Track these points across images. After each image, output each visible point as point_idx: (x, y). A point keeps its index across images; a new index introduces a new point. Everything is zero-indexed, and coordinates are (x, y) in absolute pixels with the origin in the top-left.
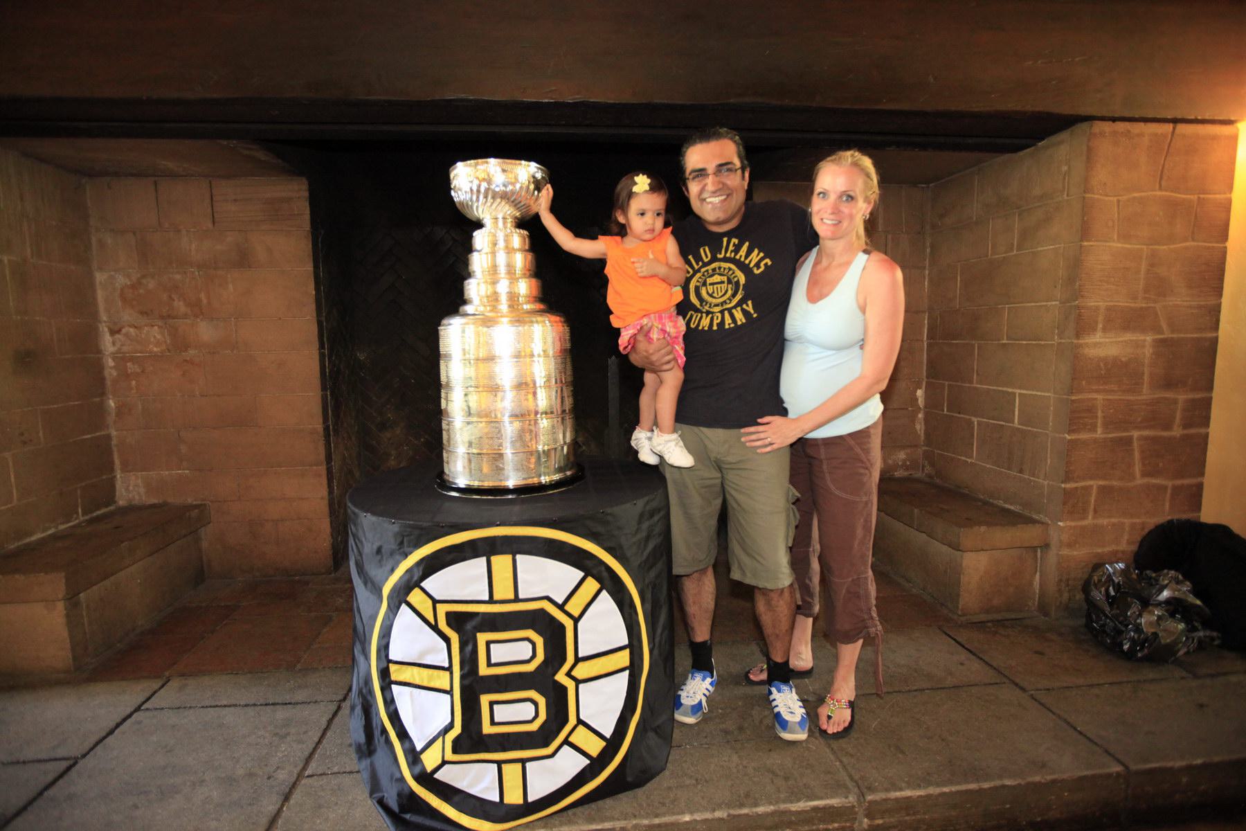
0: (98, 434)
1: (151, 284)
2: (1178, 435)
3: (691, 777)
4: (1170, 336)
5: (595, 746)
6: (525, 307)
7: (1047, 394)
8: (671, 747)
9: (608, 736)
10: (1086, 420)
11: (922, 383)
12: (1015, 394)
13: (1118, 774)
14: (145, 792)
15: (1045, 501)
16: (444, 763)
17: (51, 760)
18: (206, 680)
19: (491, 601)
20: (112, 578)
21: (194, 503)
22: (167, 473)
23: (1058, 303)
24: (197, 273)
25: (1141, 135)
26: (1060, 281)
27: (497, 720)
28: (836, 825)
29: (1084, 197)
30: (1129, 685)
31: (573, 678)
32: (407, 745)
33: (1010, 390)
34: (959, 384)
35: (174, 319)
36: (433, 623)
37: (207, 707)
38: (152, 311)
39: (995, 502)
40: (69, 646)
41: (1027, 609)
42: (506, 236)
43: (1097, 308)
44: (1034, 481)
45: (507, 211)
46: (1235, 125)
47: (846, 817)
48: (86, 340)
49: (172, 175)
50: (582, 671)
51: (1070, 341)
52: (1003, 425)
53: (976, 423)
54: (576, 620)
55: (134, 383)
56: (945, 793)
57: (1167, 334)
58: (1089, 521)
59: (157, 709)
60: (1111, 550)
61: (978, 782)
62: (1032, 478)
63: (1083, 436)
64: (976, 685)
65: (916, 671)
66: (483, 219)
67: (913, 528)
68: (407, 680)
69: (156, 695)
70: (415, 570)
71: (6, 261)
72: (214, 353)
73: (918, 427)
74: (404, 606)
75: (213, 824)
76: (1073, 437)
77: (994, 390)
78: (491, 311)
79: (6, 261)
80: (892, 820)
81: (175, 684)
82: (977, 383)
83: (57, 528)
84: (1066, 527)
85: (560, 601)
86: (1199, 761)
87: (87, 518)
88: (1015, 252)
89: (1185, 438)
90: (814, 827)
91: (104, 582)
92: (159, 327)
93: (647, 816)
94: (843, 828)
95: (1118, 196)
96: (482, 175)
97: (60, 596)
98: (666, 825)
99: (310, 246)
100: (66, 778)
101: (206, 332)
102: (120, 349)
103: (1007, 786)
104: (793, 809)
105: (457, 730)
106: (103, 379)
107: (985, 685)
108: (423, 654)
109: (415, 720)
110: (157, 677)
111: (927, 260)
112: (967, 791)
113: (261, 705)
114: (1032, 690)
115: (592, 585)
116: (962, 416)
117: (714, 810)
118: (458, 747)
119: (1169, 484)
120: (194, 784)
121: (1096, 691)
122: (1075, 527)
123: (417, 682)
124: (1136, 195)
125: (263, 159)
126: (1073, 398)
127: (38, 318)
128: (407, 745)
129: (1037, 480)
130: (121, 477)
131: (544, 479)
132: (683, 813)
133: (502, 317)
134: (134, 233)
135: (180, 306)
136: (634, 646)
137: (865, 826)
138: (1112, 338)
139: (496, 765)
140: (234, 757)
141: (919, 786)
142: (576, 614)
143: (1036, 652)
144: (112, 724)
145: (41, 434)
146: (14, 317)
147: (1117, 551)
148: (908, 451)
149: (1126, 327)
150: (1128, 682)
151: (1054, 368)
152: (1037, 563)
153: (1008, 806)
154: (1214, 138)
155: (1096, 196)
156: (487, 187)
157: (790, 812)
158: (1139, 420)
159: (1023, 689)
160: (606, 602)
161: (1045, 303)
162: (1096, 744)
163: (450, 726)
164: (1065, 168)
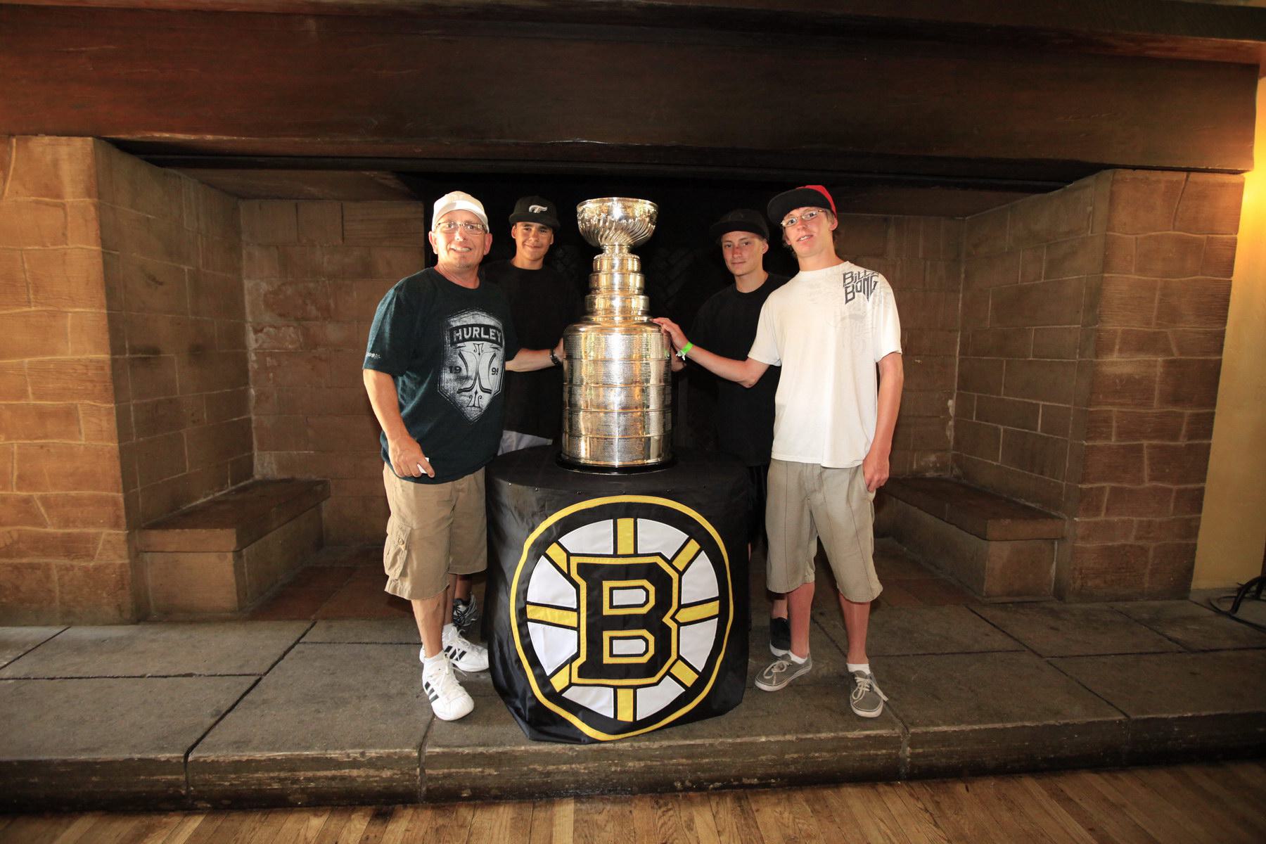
0: (242, 417)
1: (289, 291)
2: (1183, 445)
3: (763, 710)
4: (1179, 357)
5: (690, 678)
6: (636, 319)
7: (1067, 406)
8: (745, 688)
9: (700, 671)
10: (1102, 429)
11: (953, 395)
12: (1038, 405)
13: (1120, 721)
14: (322, 701)
15: (1063, 499)
16: (571, 684)
17: (240, 675)
18: (347, 623)
19: (615, 555)
20: (264, 538)
21: (318, 479)
22: (295, 452)
23: (1080, 326)
24: (327, 282)
25: (1158, 181)
26: (1083, 307)
27: (614, 653)
28: (884, 751)
29: (1106, 235)
30: (1132, 656)
31: (676, 621)
32: (538, 671)
33: (1034, 402)
34: (988, 395)
35: (306, 320)
36: (566, 570)
37: (353, 643)
38: (288, 313)
39: (1018, 500)
40: (235, 590)
41: (1043, 593)
42: (622, 261)
43: (1115, 332)
44: (1054, 482)
45: (624, 240)
46: (1242, 174)
47: (892, 746)
48: (236, 338)
49: (312, 198)
50: (683, 616)
51: (1090, 359)
52: (1026, 433)
53: (1002, 430)
54: (681, 574)
55: (271, 375)
56: (975, 730)
57: (1176, 356)
58: (1102, 518)
59: (312, 643)
60: (1119, 544)
61: (1002, 722)
62: (1053, 480)
63: (1099, 443)
64: (1001, 651)
65: (947, 639)
66: (603, 246)
67: (943, 520)
68: (541, 619)
69: (309, 632)
70: (554, 528)
71: (186, 270)
72: (338, 351)
73: (948, 433)
74: (543, 558)
75: (383, 726)
76: (1090, 444)
77: (1019, 402)
78: (606, 322)
79: (186, 268)
80: (931, 750)
81: (321, 624)
82: (1004, 395)
83: (213, 494)
84: (1082, 522)
85: (669, 558)
86: (1190, 714)
87: (233, 488)
88: (1043, 280)
89: (1189, 447)
90: (866, 752)
91: (260, 542)
92: (294, 328)
93: (731, 737)
94: (890, 755)
95: (1137, 234)
96: (604, 208)
97: (232, 549)
98: (746, 743)
99: (424, 260)
100: (257, 688)
101: (333, 332)
102: (260, 346)
103: (1027, 726)
104: (849, 736)
105: (583, 658)
106: (245, 372)
107: (1007, 651)
108: (556, 597)
109: (546, 651)
110: (305, 619)
111: (961, 287)
112: (994, 729)
113: (396, 644)
114: (1047, 657)
115: (694, 546)
116: (990, 424)
117: (785, 734)
118: (583, 672)
119: (1175, 487)
120: (359, 698)
121: (1103, 659)
122: (1089, 523)
123: (549, 621)
124: (1153, 234)
125: (393, 186)
126: (1091, 409)
127: (206, 318)
128: (538, 671)
129: (1056, 481)
130: (258, 455)
131: (652, 461)
132: (760, 735)
133: (615, 327)
134: (277, 248)
135: (312, 310)
136: (722, 598)
137: (908, 753)
138: (1129, 358)
139: (612, 689)
140: (385, 681)
141: (954, 724)
142: (681, 570)
143: (1052, 628)
144: (281, 652)
145: (205, 416)
146: (190, 316)
147: (1125, 546)
148: (939, 454)
149: (1140, 349)
150: (1131, 654)
151: (1075, 383)
152: (1054, 552)
153: (1027, 743)
154: (1223, 185)
155: (1115, 234)
156: (613, 220)
157: (847, 738)
158: (1149, 430)
159: (1040, 656)
160: (704, 561)
161: (1069, 326)
162: (1103, 699)
163: (577, 656)
164: (1090, 209)
